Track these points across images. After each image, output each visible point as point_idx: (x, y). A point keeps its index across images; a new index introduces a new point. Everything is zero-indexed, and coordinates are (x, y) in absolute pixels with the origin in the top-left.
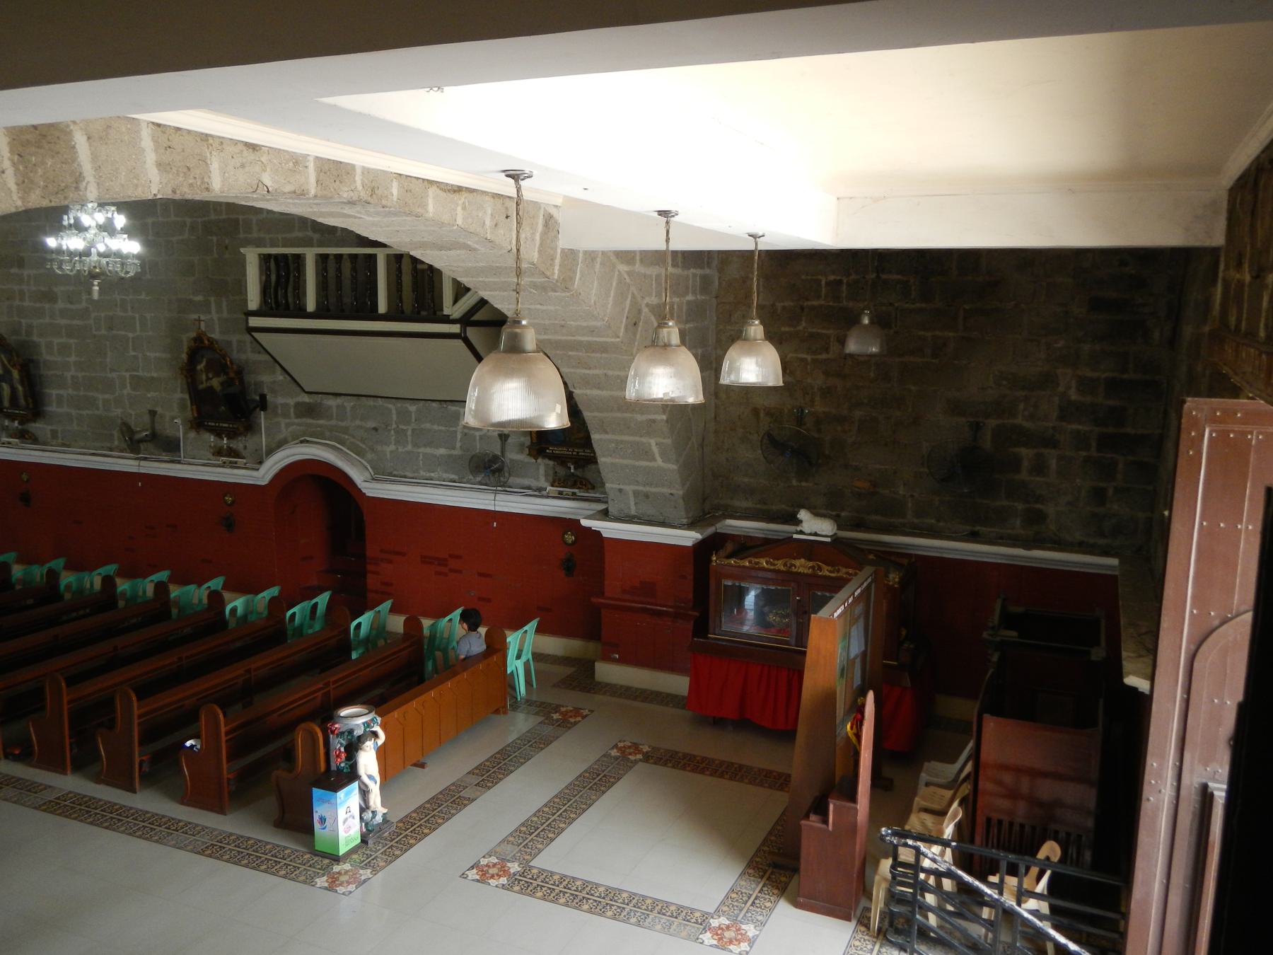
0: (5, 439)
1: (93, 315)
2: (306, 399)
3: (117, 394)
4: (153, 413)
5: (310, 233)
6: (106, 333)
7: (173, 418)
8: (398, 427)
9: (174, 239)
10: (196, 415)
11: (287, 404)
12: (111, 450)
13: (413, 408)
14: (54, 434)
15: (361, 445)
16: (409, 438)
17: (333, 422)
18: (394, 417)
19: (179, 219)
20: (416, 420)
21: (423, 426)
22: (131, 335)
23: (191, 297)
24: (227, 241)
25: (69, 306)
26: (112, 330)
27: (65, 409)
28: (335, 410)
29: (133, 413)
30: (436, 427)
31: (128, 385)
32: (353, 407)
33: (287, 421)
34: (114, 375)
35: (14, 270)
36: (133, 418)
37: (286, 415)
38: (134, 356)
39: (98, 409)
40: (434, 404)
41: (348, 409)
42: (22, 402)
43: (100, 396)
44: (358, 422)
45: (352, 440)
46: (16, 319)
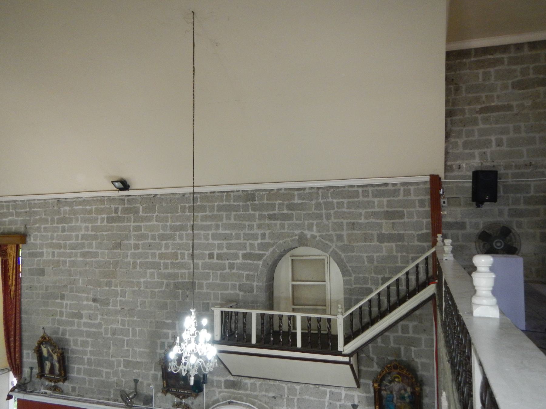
0: (43, 390)
1: (104, 327)
2: (232, 378)
3: (115, 369)
4: (136, 381)
5: (238, 292)
6: (111, 336)
7: (149, 385)
8: (288, 397)
9: (157, 290)
10: (165, 385)
11: (220, 381)
12: (108, 400)
13: (298, 387)
14: (74, 389)
15: (265, 405)
16: (296, 404)
17: (249, 392)
18: (286, 391)
19: (160, 280)
20: (299, 393)
21: (304, 397)
22: (126, 338)
23: (164, 320)
24: (188, 293)
25: (89, 321)
26: (115, 335)
27: (82, 376)
28: (249, 386)
29: (124, 380)
30: (312, 398)
31: (122, 365)
32: (261, 385)
33: (220, 390)
34: (114, 359)
35: (58, 301)
36: (124, 383)
37: (219, 387)
38: (127, 350)
39: (102, 377)
40: (311, 386)
41: (258, 385)
42: (57, 372)
43: (105, 370)
44: (263, 393)
45: (260, 402)
46: (56, 326)
